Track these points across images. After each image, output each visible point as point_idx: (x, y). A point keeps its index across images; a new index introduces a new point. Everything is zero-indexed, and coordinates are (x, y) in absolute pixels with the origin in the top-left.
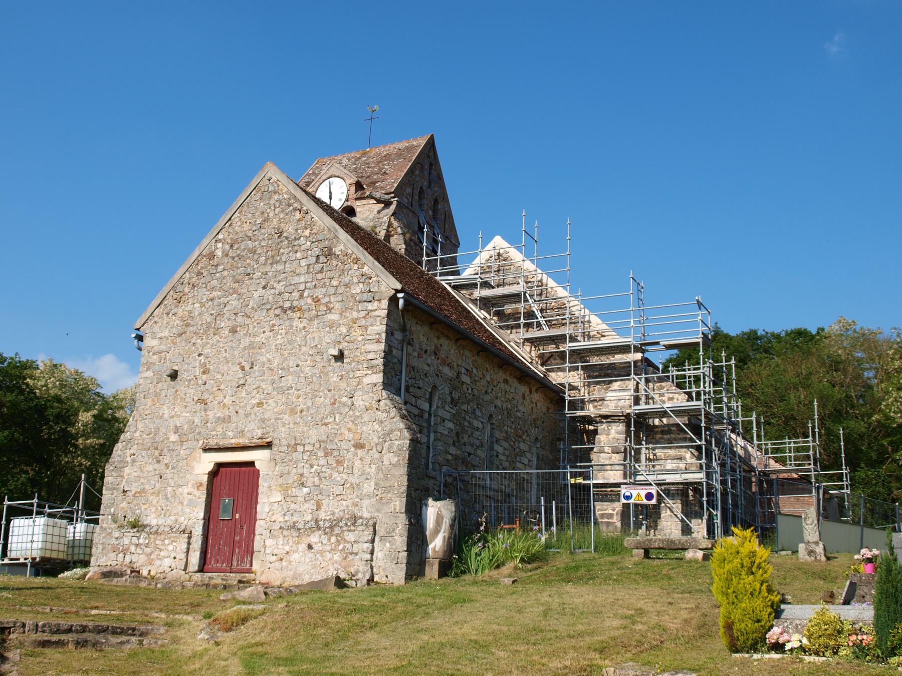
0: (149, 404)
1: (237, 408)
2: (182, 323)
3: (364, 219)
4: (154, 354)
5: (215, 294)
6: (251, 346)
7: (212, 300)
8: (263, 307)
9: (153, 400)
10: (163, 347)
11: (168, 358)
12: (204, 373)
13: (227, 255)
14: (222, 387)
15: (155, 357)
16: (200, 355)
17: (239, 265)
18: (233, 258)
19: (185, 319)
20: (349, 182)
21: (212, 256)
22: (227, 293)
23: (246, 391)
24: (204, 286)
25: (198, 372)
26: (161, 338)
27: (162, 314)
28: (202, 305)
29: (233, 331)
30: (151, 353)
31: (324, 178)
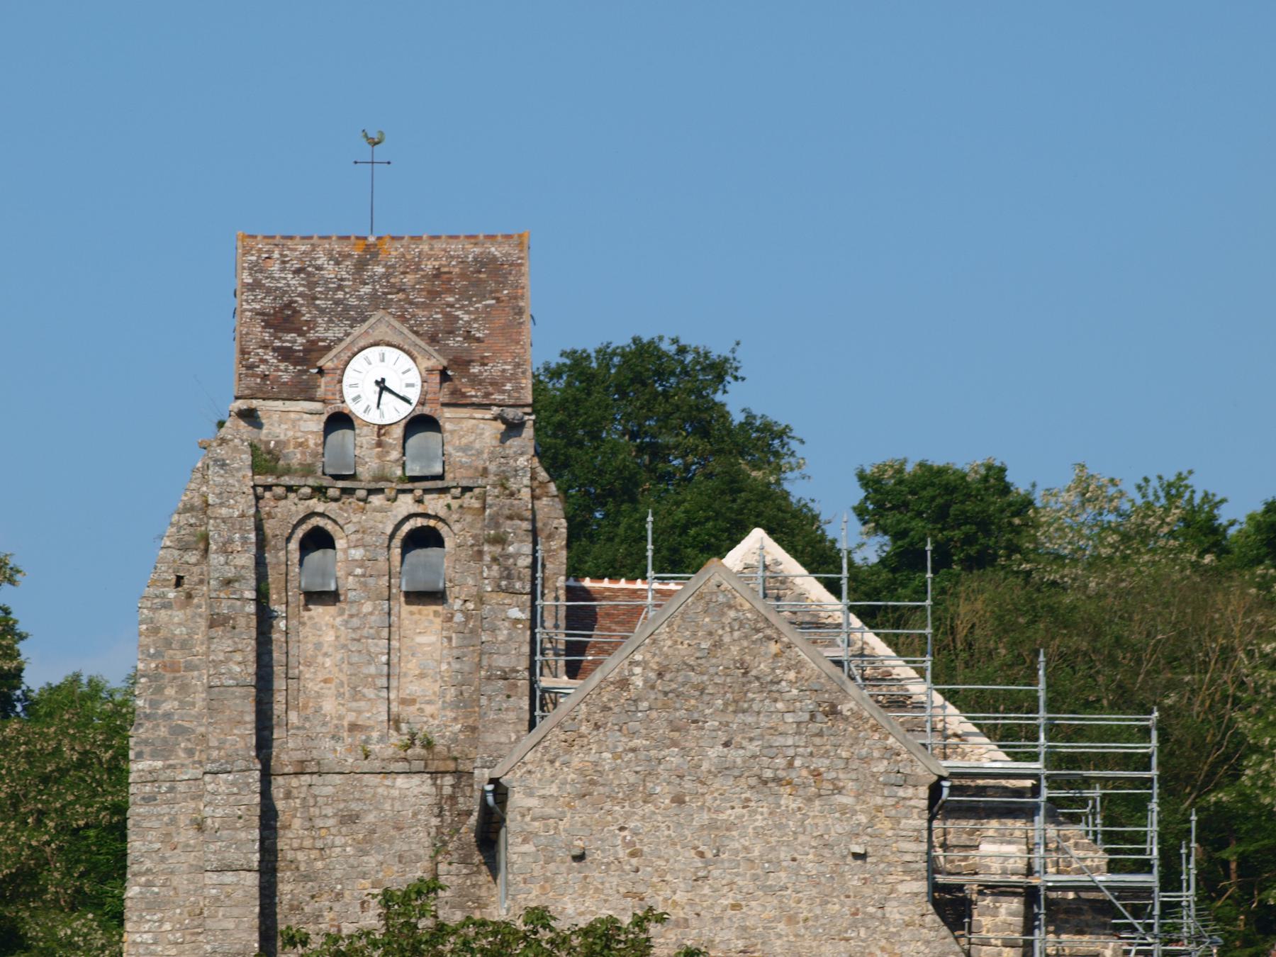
0: (534, 893)
1: (698, 909)
2: (582, 779)
3: (465, 449)
4: (533, 819)
5: (637, 742)
6: (713, 825)
7: (633, 750)
8: (728, 772)
9: (542, 887)
10: (549, 811)
11: (561, 828)
12: (633, 855)
13: (653, 687)
14: (668, 878)
15: (536, 824)
16: (622, 829)
17: (678, 705)
18: (666, 694)
19: (587, 773)
20: (431, 363)
21: (624, 683)
22: (661, 744)
23: (711, 887)
24: (616, 728)
25: (622, 853)
26: (543, 797)
27: (541, 760)
28: (616, 756)
29: (679, 800)
30: (528, 819)
31: (362, 343)
